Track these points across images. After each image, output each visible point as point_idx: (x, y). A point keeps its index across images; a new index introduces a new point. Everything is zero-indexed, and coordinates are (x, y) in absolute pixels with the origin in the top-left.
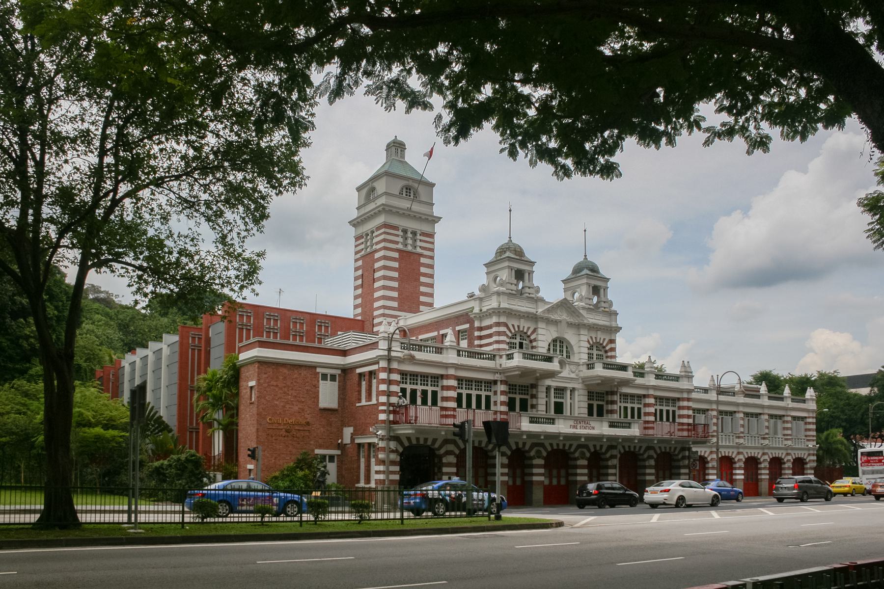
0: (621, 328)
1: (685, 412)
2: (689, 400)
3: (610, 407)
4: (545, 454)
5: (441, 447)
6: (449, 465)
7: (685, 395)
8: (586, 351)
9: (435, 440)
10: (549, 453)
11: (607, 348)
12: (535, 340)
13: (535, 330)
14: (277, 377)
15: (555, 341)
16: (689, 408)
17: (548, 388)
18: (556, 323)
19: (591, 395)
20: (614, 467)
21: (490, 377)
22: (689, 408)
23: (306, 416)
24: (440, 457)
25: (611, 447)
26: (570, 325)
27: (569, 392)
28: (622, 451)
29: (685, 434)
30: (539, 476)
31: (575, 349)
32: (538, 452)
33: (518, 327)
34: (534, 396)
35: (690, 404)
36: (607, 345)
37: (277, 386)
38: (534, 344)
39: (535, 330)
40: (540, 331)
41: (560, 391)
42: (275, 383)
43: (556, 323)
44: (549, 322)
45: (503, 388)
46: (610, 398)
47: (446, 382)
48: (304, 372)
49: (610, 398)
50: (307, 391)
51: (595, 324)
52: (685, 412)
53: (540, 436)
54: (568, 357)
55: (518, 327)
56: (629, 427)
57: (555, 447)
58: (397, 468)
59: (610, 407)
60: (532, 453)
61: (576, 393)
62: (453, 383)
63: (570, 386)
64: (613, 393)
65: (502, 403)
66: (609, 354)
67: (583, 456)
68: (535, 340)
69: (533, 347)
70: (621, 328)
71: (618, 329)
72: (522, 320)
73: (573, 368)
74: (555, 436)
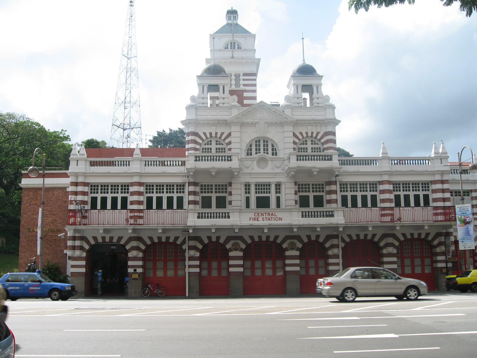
0: (340, 121)
1: (439, 195)
2: (443, 182)
3: (328, 197)
4: (243, 246)
5: (127, 242)
6: (135, 259)
7: (438, 177)
8: (292, 146)
9: (120, 238)
10: (248, 246)
11: (322, 141)
12: (230, 143)
13: (229, 135)
14: (36, 198)
15: (258, 141)
16: (443, 191)
17: (247, 186)
18: (254, 124)
19: (301, 187)
20: (336, 256)
21: (179, 180)
22: (443, 191)
23: (58, 225)
24: (127, 252)
25: (329, 238)
26: (270, 124)
27: (273, 188)
28: (348, 240)
29: (440, 218)
30: (236, 266)
31: (280, 146)
32: (235, 244)
33: (211, 134)
34: (230, 194)
35: (446, 186)
36: (322, 137)
37: (36, 204)
38: (229, 147)
39: (229, 135)
40: (233, 134)
41: (263, 187)
42: (34, 203)
43: (254, 124)
44: (242, 125)
45: (192, 188)
46: (328, 188)
47: (132, 189)
48: (56, 193)
49: (328, 188)
50: (59, 206)
51: (297, 120)
52: (439, 195)
53: (210, 229)
54: (275, 153)
55: (211, 134)
56: (332, 216)
57: (257, 239)
58: (83, 263)
59: (328, 197)
60: (228, 246)
61: (283, 187)
62: (142, 189)
63: (273, 180)
64: (330, 183)
65: (195, 203)
66: (325, 146)
67: (292, 247)
68: (230, 143)
69: (230, 149)
70: (340, 121)
71: (336, 122)
72: (214, 128)
73: (277, 163)
74: (231, 229)
